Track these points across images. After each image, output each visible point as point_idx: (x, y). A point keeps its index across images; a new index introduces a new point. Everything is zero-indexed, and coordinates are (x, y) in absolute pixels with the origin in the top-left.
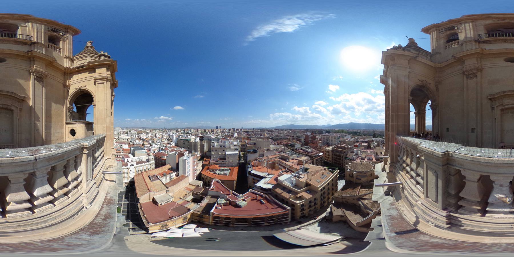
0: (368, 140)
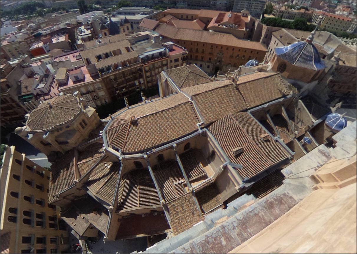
0: (68, 24)
